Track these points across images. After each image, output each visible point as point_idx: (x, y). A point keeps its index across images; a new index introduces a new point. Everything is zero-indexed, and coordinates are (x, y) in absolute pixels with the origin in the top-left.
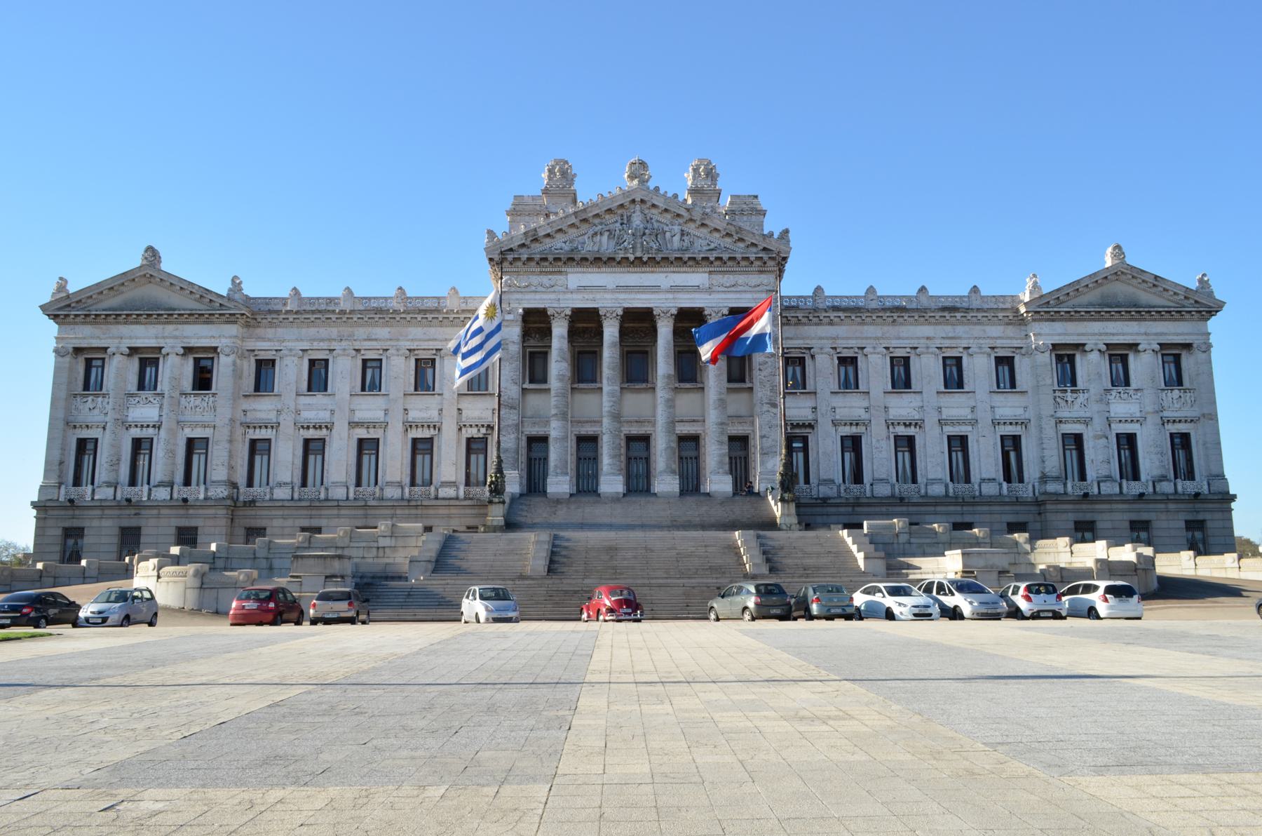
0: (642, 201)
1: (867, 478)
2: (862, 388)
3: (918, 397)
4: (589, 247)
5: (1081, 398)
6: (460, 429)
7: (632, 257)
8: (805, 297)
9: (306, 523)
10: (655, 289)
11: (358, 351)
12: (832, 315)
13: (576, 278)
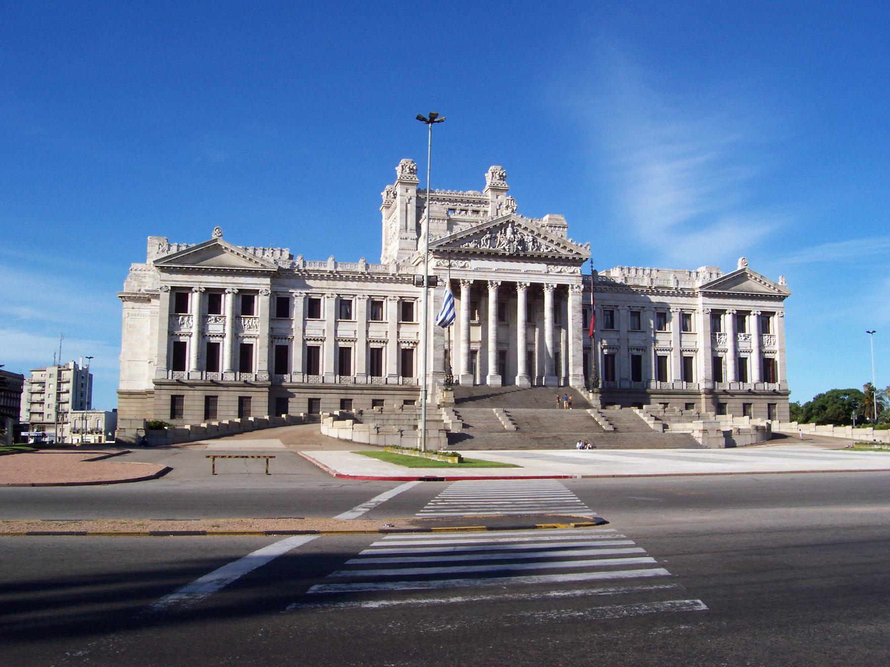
0: (513, 222)
1: (617, 378)
2: (616, 328)
3: (644, 334)
4: (485, 247)
5: (723, 338)
6: (398, 343)
7: (507, 254)
8: (588, 276)
9: (312, 396)
10: (517, 272)
11: (339, 295)
12: (603, 287)
13: (474, 264)
